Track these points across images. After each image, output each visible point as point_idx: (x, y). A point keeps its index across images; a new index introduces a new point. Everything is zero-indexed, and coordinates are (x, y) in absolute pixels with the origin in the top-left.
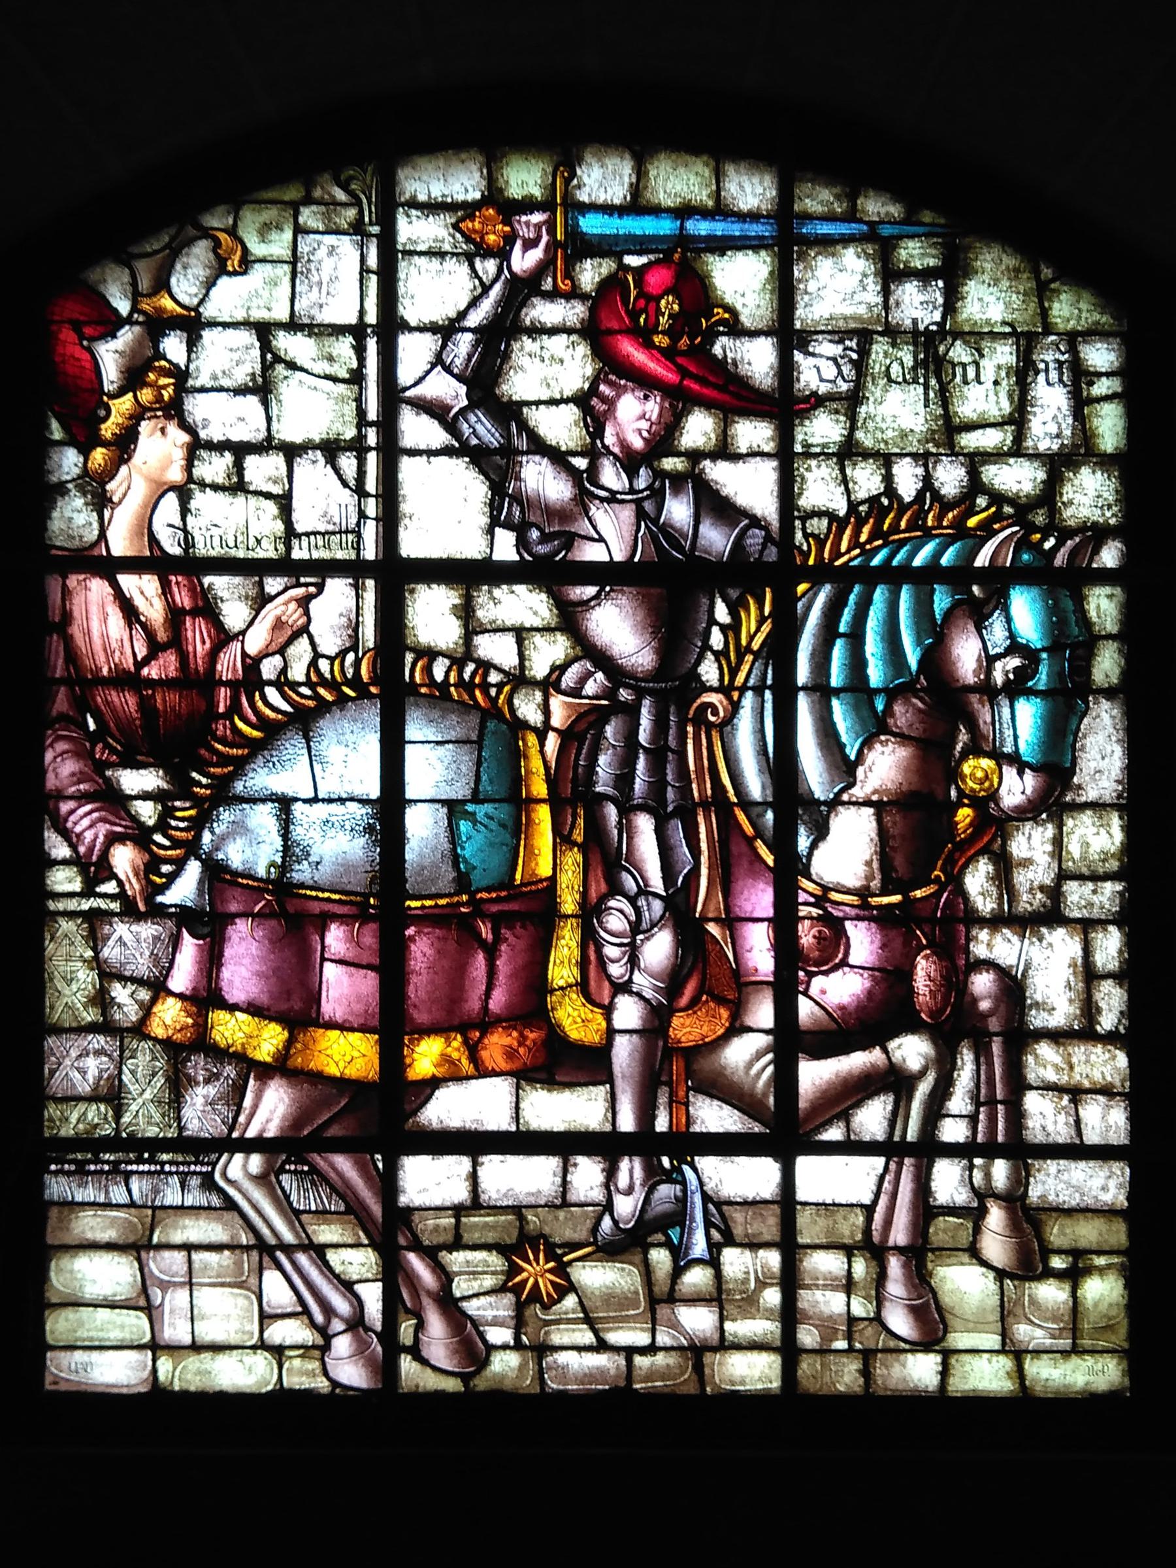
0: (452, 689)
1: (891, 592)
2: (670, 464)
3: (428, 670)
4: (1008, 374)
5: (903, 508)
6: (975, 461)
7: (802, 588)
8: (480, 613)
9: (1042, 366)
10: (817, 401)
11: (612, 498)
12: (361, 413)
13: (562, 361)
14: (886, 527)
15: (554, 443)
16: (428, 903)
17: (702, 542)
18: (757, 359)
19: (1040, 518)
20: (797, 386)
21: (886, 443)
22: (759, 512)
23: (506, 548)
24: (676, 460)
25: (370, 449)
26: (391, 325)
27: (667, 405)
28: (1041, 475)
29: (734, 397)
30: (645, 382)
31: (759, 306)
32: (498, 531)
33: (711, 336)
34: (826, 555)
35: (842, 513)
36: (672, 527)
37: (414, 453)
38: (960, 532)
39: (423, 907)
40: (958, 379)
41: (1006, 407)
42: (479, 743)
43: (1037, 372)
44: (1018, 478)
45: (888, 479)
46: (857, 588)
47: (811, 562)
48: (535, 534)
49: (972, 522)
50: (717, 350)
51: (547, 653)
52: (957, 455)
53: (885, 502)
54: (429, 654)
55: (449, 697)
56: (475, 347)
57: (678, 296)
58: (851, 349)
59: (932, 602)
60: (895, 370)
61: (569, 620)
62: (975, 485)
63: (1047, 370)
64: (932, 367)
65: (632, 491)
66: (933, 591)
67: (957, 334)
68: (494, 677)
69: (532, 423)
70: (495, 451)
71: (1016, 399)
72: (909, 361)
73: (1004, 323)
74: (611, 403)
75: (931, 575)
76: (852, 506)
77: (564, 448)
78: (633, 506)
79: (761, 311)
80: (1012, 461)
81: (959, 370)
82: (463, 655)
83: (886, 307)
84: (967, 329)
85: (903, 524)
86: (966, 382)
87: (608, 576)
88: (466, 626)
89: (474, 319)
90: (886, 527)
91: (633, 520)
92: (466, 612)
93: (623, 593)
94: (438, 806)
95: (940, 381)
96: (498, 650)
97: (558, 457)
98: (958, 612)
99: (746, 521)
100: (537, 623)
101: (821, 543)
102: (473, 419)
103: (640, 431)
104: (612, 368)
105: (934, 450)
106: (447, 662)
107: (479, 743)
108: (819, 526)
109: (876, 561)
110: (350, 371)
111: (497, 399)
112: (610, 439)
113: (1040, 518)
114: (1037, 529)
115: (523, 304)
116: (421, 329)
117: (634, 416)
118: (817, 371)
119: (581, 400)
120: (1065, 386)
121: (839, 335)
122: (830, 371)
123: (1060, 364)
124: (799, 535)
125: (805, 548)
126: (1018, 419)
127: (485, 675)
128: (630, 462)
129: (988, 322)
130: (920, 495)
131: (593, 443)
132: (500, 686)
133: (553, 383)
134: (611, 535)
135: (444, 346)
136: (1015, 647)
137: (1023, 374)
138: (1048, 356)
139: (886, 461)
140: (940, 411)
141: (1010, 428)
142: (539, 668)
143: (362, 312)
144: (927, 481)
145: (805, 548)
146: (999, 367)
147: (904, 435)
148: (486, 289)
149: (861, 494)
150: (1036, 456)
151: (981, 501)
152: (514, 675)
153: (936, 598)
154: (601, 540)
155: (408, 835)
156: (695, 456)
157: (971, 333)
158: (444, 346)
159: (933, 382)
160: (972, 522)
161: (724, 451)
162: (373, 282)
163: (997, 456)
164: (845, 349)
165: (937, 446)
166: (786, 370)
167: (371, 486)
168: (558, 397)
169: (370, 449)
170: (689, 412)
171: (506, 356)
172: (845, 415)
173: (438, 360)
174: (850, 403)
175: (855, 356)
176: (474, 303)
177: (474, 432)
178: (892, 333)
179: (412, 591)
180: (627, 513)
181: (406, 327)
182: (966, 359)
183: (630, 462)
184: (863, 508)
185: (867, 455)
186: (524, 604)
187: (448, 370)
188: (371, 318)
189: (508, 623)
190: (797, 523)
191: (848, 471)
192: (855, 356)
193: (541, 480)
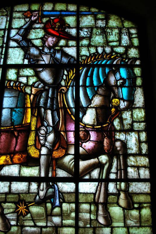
0: (14, 87)
1: (97, 69)
2: (57, 48)
3: (10, 84)
4: (117, 34)
5: (99, 55)
6: (112, 47)
7: (80, 69)
8: (20, 74)
9: (123, 33)
10: (83, 38)
11: (46, 54)
12: (3, 42)
13: (39, 33)
14: (96, 58)
15: (36, 45)
16: (5, 128)
17: (62, 61)
18: (73, 32)
19: (125, 56)
20: (80, 36)
21: (96, 44)
22: (73, 56)
23: (26, 62)
24: (58, 47)
25: (4, 47)
26: (10, 28)
27: (57, 39)
28: (124, 49)
29: (69, 37)
30: (53, 36)
31: (73, 24)
32: (25, 60)
33: (65, 28)
34: (85, 62)
35: (88, 56)
36: (57, 58)
37: (11, 47)
38: (110, 59)
39: (4, 129)
40: (109, 34)
41: (117, 39)
42: (18, 97)
43: (122, 34)
44: (120, 50)
45: (97, 50)
46: (91, 68)
47: (83, 63)
48: (32, 60)
49: (112, 57)
50: (66, 30)
51: (32, 80)
52: (109, 46)
53: (96, 54)
54: (10, 81)
55: (13, 88)
56: (24, 31)
57: (59, 23)
58: (90, 30)
59: (105, 71)
60: (97, 33)
61: (37, 74)
62: (112, 51)
63: (124, 33)
64: (104, 33)
65: (50, 52)
66: (105, 69)
67: (108, 28)
68: (22, 85)
69: (33, 42)
70: (26, 47)
71: (119, 37)
72: (100, 32)
73: (116, 26)
74: (47, 39)
75: (104, 66)
76: (90, 54)
77: (38, 46)
78: (50, 55)
79: (74, 25)
80: (119, 47)
81: (109, 33)
82: (17, 80)
83: (96, 24)
84: (110, 27)
85: (100, 57)
86: (110, 35)
87: (45, 67)
88: (17, 76)
89: (24, 27)
90: (96, 58)
91: (50, 57)
92: (18, 74)
93: (47, 69)
94: (9, 109)
95: (105, 35)
96: (23, 80)
97: (37, 47)
98: (110, 72)
99: (71, 57)
100: (31, 75)
101: (84, 60)
102: (22, 42)
103: (52, 43)
104: (47, 34)
105: (105, 45)
106: (13, 82)
107: (18, 97)
108: (84, 58)
109: (95, 63)
110: (2, 35)
111: (27, 39)
112: (46, 44)
113: (125, 56)
114: (124, 58)
115: (33, 25)
116: (15, 29)
117: (51, 40)
118: (83, 34)
119: (41, 38)
120: (127, 36)
121: (87, 28)
122: (86, 33)
123: (126, 32)
124: (80, 59)
125: (81, 61)
126: (120, 40)
127: (20, 84)
128: (50, 48)
129: (113, 26)
130: (102, 53)
131: (43, 45)
132: (23, 86)
133: (37, 36)
134: (46, 59)
135: (19, 31)
136: (121, 78)
137: (120, 34)
138: (124, 31)
139: (96, 47)
140: (106, 39)
141: (118, 42)
142: (31, 83)
143: (6, 27)
144: (104, 51)
145: (81, 61)
146: (116, 33)
147: (99, 43)
148: (27, 23)
149: (92, 53)
150: (123, 46)
151: (114, 54)
152: (26, 84)
153: (106, 70)
154: (44, 61)
155: (3, 114)
156: (62, 47)
157: (110, 28)
158: (19, 31)
159: (104, 35)
160: (112, 57)
161: (67, 46)
162: (8, 22)
163: (116, 46)
164: (89, 30)
165: (105, 45)
166: (78, 33)
167: (3, 53)
168: (38, 38)
169: (4, 47)
170: (61, 40)
171: (29, 32)
172: (89, 40)
173: (17, 33)
174: (90, 38)
175: (90, 31)
176: (24, 25)
177: (23, 44)
178: (97, 28)
179: (8, 70)
180: (49, 56)
181: (13, 29)
182: (109, 31)
183: (50, 48)
184: (92, 55)
185: (93, 46)
186: (28, 72)
187: (19, 35)
188: (7, 27)
189: (25, 75)
190: (80, 57)
191: (89, 49)
192: (90, 31)
193: (34, 51)
